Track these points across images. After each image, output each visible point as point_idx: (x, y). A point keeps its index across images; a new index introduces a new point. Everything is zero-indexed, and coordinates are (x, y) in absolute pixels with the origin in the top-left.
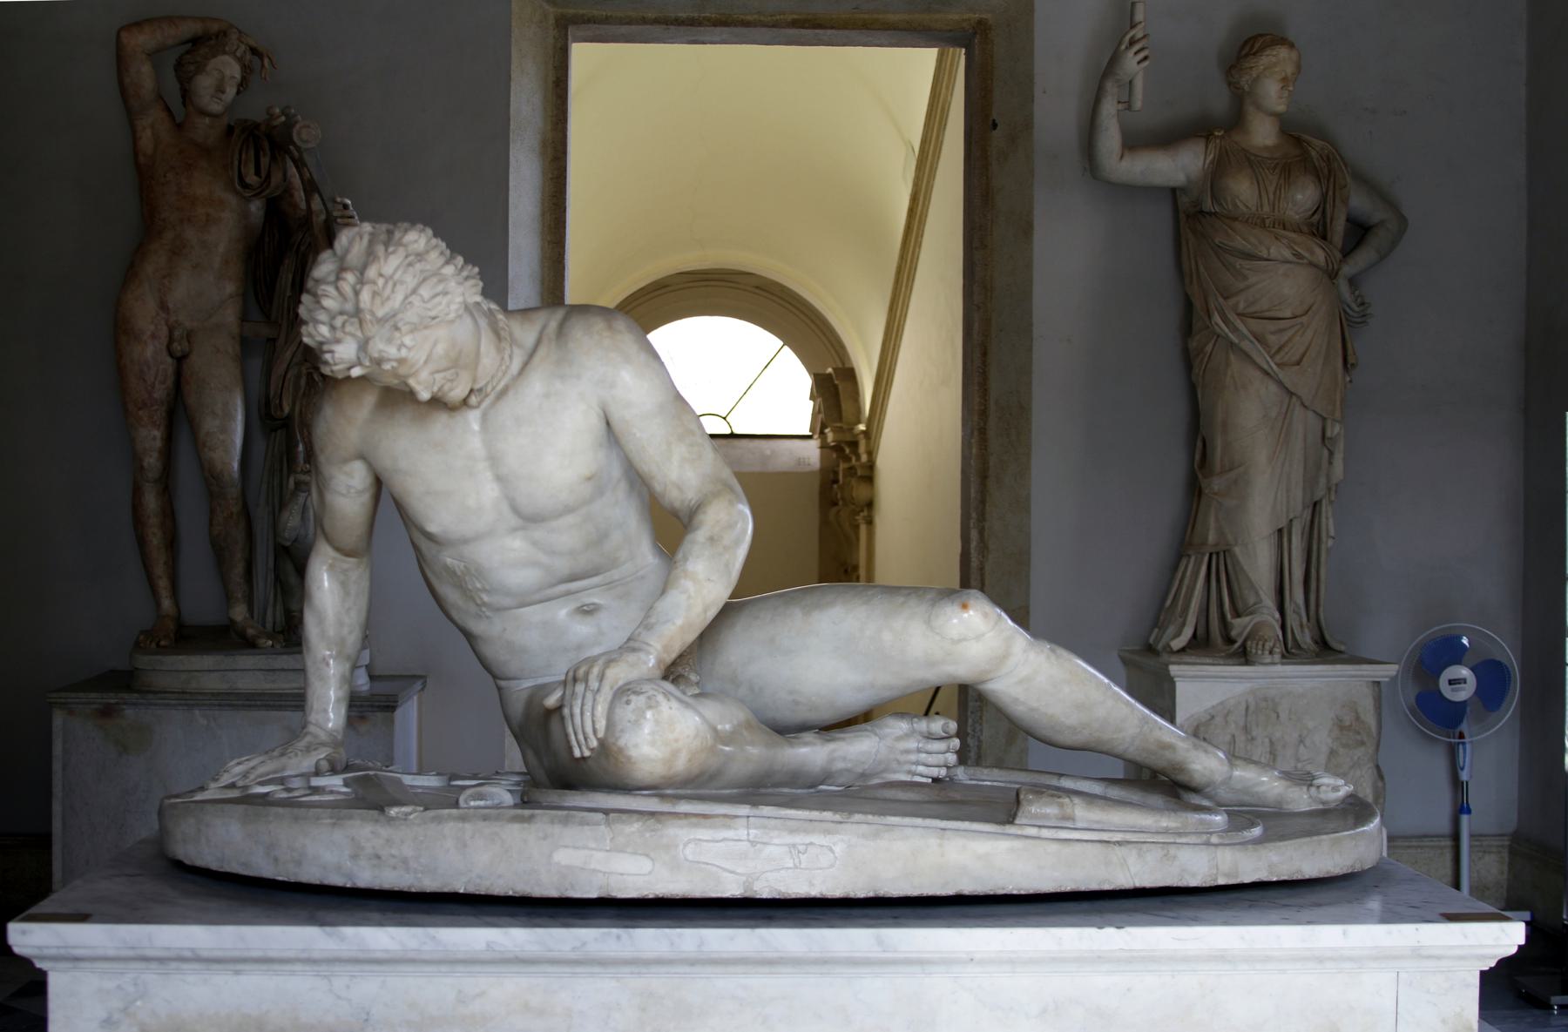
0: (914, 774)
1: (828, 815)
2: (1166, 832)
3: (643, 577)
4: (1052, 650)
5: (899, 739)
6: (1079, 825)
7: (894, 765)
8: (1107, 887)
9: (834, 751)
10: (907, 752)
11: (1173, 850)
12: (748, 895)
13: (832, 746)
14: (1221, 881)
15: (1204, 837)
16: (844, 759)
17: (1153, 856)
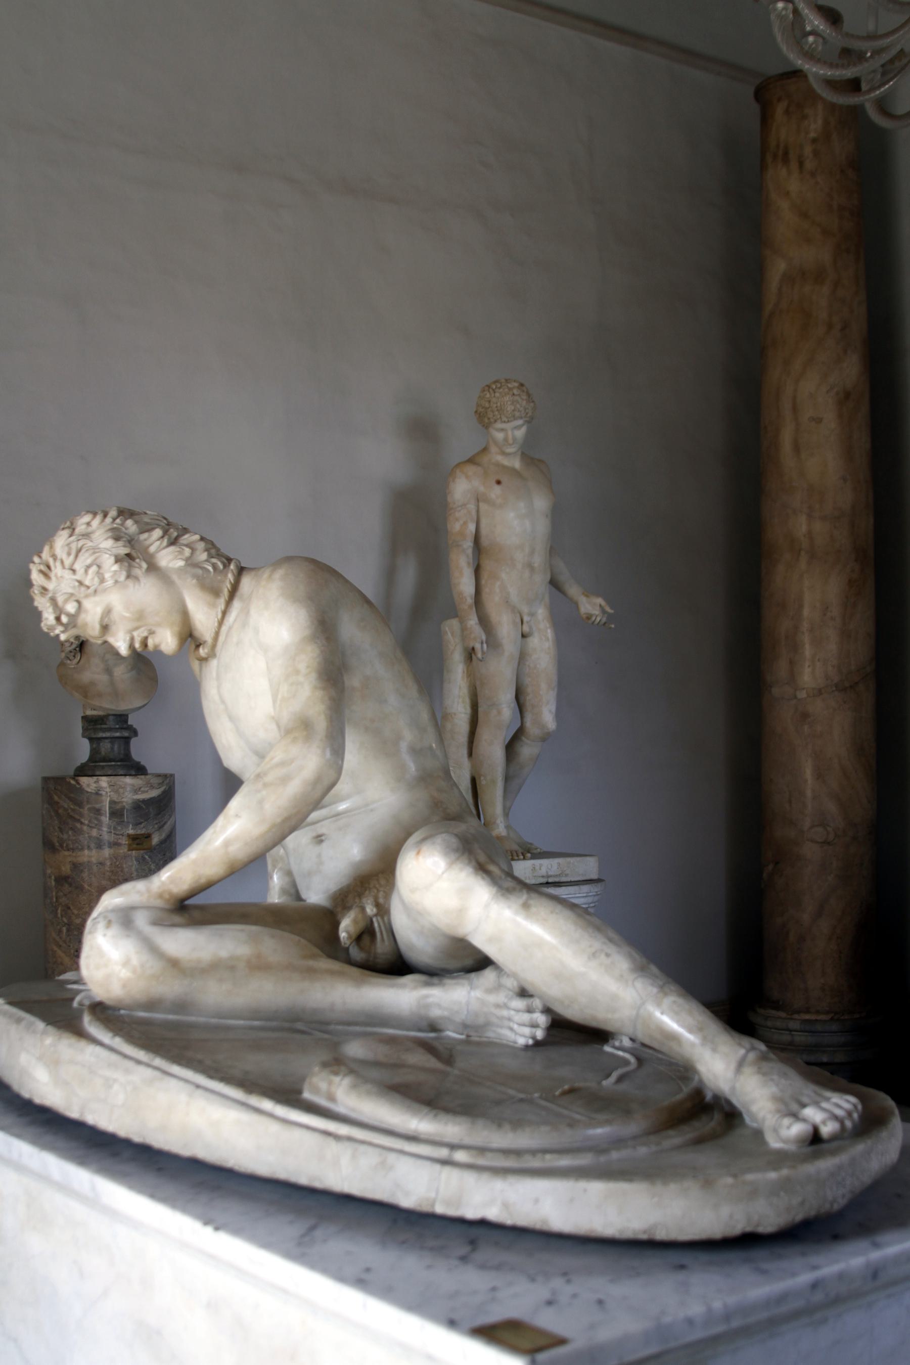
0: (516, 1034)
1: (141, 1055)
2: (413, 1138)
3: (372, 810)
4: (526, 906)
5: (489, 991)
6: (340, 1109)
7: (495, 1020)
8: (317, 1184)
9: (427, 996)
10: (498, 1006)
11: (392, 1157)
12: (82, 1119)
13: (425, 991)
14: (439, 1209)
15: (443, 1153)
16: (439, 1006)
17: (368, 1159)
